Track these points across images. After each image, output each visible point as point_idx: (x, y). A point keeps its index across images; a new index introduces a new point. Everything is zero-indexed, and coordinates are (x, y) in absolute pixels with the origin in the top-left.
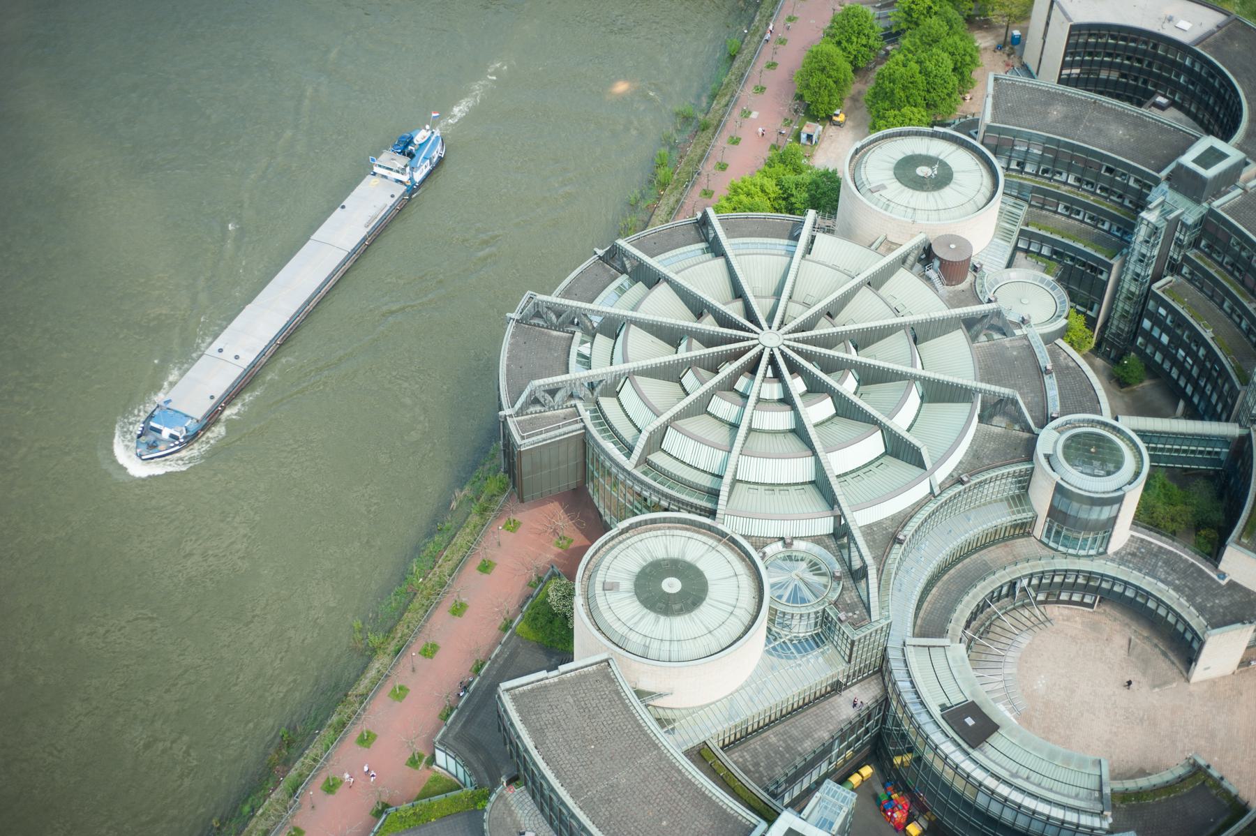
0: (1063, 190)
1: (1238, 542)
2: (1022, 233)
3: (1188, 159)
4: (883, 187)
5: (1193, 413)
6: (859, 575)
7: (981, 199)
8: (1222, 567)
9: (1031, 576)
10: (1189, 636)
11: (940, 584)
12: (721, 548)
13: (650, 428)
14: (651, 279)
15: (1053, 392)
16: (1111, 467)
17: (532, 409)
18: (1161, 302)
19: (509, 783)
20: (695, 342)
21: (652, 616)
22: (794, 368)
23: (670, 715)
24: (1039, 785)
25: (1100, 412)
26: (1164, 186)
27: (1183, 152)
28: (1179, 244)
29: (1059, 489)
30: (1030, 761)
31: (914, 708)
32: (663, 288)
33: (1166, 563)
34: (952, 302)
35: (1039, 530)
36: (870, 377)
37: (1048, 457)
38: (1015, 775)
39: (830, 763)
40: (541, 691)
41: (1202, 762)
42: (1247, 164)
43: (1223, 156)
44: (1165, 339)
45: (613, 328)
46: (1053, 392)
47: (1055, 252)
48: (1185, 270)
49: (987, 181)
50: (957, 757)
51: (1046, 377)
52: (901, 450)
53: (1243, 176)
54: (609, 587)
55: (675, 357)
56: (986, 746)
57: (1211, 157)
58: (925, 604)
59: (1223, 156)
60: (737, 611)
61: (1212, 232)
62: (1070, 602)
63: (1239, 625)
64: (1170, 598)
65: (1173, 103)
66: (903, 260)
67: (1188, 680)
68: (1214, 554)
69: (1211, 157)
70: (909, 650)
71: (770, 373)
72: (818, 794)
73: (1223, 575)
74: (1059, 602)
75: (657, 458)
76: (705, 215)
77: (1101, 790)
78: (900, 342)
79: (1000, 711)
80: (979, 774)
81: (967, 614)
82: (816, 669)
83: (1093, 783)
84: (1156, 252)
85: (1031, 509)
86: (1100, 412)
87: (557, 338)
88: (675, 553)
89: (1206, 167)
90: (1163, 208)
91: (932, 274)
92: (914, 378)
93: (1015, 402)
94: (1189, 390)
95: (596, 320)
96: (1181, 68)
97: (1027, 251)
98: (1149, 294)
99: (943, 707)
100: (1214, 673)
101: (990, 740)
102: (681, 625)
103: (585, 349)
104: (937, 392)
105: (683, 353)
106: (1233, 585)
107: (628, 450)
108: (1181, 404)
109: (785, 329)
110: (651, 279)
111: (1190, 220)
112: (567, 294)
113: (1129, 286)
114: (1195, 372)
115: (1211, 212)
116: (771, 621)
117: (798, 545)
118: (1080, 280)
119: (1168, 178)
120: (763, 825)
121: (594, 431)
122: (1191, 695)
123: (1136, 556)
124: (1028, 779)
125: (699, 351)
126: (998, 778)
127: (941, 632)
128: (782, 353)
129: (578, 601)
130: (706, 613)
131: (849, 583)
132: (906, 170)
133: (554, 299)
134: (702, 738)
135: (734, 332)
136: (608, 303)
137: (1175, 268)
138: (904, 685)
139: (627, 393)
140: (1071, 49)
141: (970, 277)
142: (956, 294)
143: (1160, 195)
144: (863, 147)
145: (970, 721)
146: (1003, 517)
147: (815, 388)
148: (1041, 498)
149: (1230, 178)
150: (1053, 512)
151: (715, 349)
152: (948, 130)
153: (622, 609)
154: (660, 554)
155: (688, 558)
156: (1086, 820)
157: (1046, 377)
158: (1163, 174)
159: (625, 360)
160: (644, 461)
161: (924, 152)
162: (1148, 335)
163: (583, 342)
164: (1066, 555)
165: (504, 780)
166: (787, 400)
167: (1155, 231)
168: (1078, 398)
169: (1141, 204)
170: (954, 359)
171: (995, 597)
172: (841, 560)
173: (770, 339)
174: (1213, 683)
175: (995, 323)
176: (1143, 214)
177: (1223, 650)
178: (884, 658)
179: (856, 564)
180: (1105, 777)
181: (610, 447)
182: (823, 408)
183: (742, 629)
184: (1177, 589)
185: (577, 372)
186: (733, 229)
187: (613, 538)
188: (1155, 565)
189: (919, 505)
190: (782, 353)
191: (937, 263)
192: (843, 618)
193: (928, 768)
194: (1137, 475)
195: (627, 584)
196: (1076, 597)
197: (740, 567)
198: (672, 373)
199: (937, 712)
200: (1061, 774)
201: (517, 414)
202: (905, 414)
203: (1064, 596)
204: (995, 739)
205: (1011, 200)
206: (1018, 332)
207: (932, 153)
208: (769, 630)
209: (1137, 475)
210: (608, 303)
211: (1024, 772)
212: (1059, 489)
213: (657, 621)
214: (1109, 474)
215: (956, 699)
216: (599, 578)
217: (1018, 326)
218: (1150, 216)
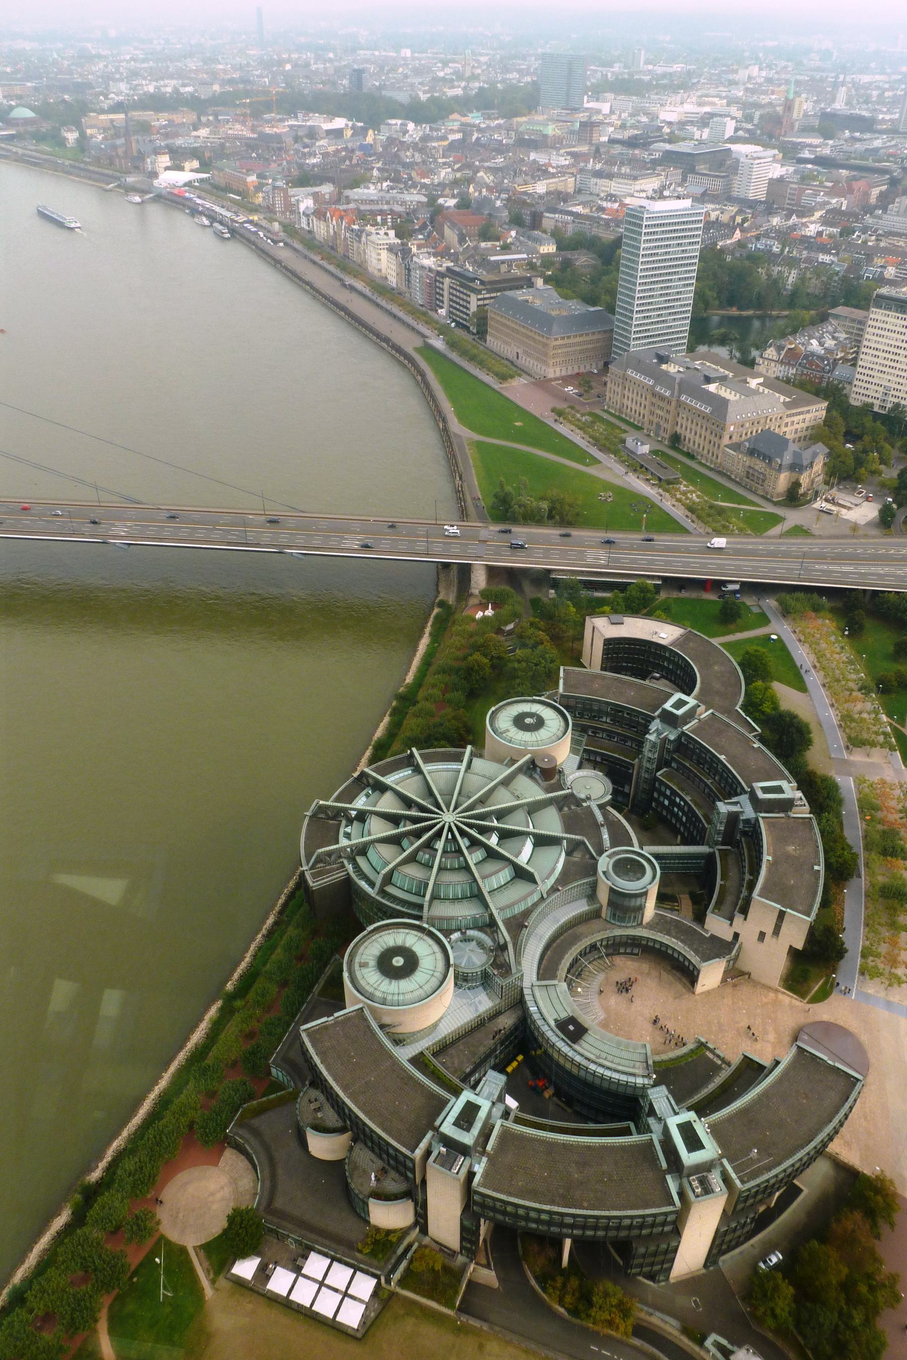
0: (605, 726)
1: (713, 912)
2: (585, 750)
3: (668, 706)
4: (508, 731)
5: (685, 842)
6: (503, 948)
7: (560, 733)
8: (706, 926)
9: (602, 940)
10: (691, 968)
11: (551, 949)
12: (426, 938)
13: (383, 872)
14: (382, 788)
15: (606, 836)
16: (639, 875)
17: (319, 865)
18: (662, 783)
19: (310, 1085)
20: (408, 822)
21: (387, 981)
22: (463, 833)
23: (401, 1037)
24: (612, 1062)
25: (632, 846)
26: (657, 721)
27: (666, 701)
28: (668, 751)
29: (611, 890)
30: (606, 1048)
31: (540, 1023)
32: (388, 795)
33: (676, 926)
34: (548, 790)
35: (605, 912)
36: (505, 835)
37: (604, 873)
38: (598, 1057)
39: (496, 1058)
40: (324, 1028)
41: (703, 1040)
43: (686, 703)
44: (666, 802)
45: (362, 817)
46: (606, 836)
47: (602, 759)
48: (674, 765)
49: (562, 723)
50: (565, 1049)
51: (602, 828)
52: (521, 874)
53: (698, 713)
54: (364, 965)
55: (397, 831)
56: (582, 1042)
58: (544, 962)
59: (686, 703)
60: (436, 974)
61: (684, 746)
62: (625, 953)
63: (717, 960)
64: (679, 947)
65: (662, 677)
66: (520, 770)
67: (694, 993)
68: (700, 918)
69: (680, 704)
70: (536, 990)
71: (450, 836)
72: (484, 1078)
73: (707, 931)
74: (619, 954)
75: (390, 889)
76: (412, 753)
77: (647, 1062)
78: (520, 815)
79: (585, 1020)
80: (578, 1058)
81: (568, 965)
82: (483, 1003)
83: (643, 1059)
84: (656, 756)
85: (599, 902)
86: (632, 846)
87: (333, 824)
88: (399, 942)
89: (678, 709)
90: (656, 732)
91: (537, 777)
92: (527, 834)
93: (584, 843)
94: (682, 829)
95: (354, 813)
96: (665, 658)
97: (588, 760)
98: (656, 779)
99: (556, 1021)
100: (705, 988)
101: (585, 1037)
102: (406, 985)
103: (348, 830)
104: (542, 841)
105: (402, 829)
106: (713, 937)
107: (372, 884)
108: (679, 837)
109: (459, 809)
110: (382, 788)
111: (672, 737)
112: (336, 800)
113: (644, 775)
114: (684, 819)
115: (683, 733)
116: (456, 977)
117: (470, 933)
118: (617, 773)
119: (659, 716)
120: (453, 1099)
121: (353, 876)
122: (696, 1001)
123: (659, 924)
124: (606, 1059)
125: (410, 827)
126: (589, 1060)
127: (554, 977)
128: (455, 825)
129: (346, 975)
130: (419, 976)
131: (499, 953)
132: (519, 722)
133: (329, 803)
134: (420, 1050)
135: (429, 815)
136: (361, 802)
137: (667, 764)
138: (533, 1009)
139: (371, 853)
140: (606, 652)
141: (557, 777)
142: (551, 785)
143: (655, 725)
144: (496, 710)
145: (571, 1028)
146: (581, 907)
147: (475, 843)
148: (603, 896)
149: (691, 714)
150: (610, 903)
151: (418, 825)
152: (542, 698)
153: (371, 978)
154: (391, 943)
155: (407, 945)
156: (640, 1081)
157: (602, 828)
158: (657, 713)
159: (370, 835)
160: (382, 892)
161: (528, 711)
162: (657, 800)
163: (347, 826)
164: (620, 927)
165: (307, 1083)
166: (459, 851)
167: (654, 745)
168: (620, 838)
169: (647, 731)
170: (551, 823)
171: (583, 954)
172: (494, 940)
173: (449, 818)
174: (708, 993)
175: (571, 799)
176: (647, 736)
177: (711, 975)
178: (522, 995)
179: (502, 942)
180: (649, 1053)
181: (363, 884)
182: (479, 855)
183: (438, 983)
184: (682, 941)
185: (344, 842)
186: (427, 759)
187: (364, 937)
188: (670, 930)
189: (535, 905)
190: (455, 825)
191: (538, 770)
192: (496, 973)
193: (550, 1057)
194: (654, 877)
195: (373, 963)
196: (628, 950)
197: (436, 948)
198: (395, 841)
199: (552, 1023)
200: (624, 1054)
201: (311, 869)
202: (525, 853)
203: (622, 951)
204: (586, 1037)
205: (577, 733)
206: (585, 804)
207: (533, 710)
208: (456, 984)
209: (654, 877)
210: (361, 802)
211: (604, 1055)
212: (611, 890)
213: (390, 983)
214: (638, 879)
215: (563, 1015)
216: (357, 960)
217: (584, 801)
218: (652, 737)
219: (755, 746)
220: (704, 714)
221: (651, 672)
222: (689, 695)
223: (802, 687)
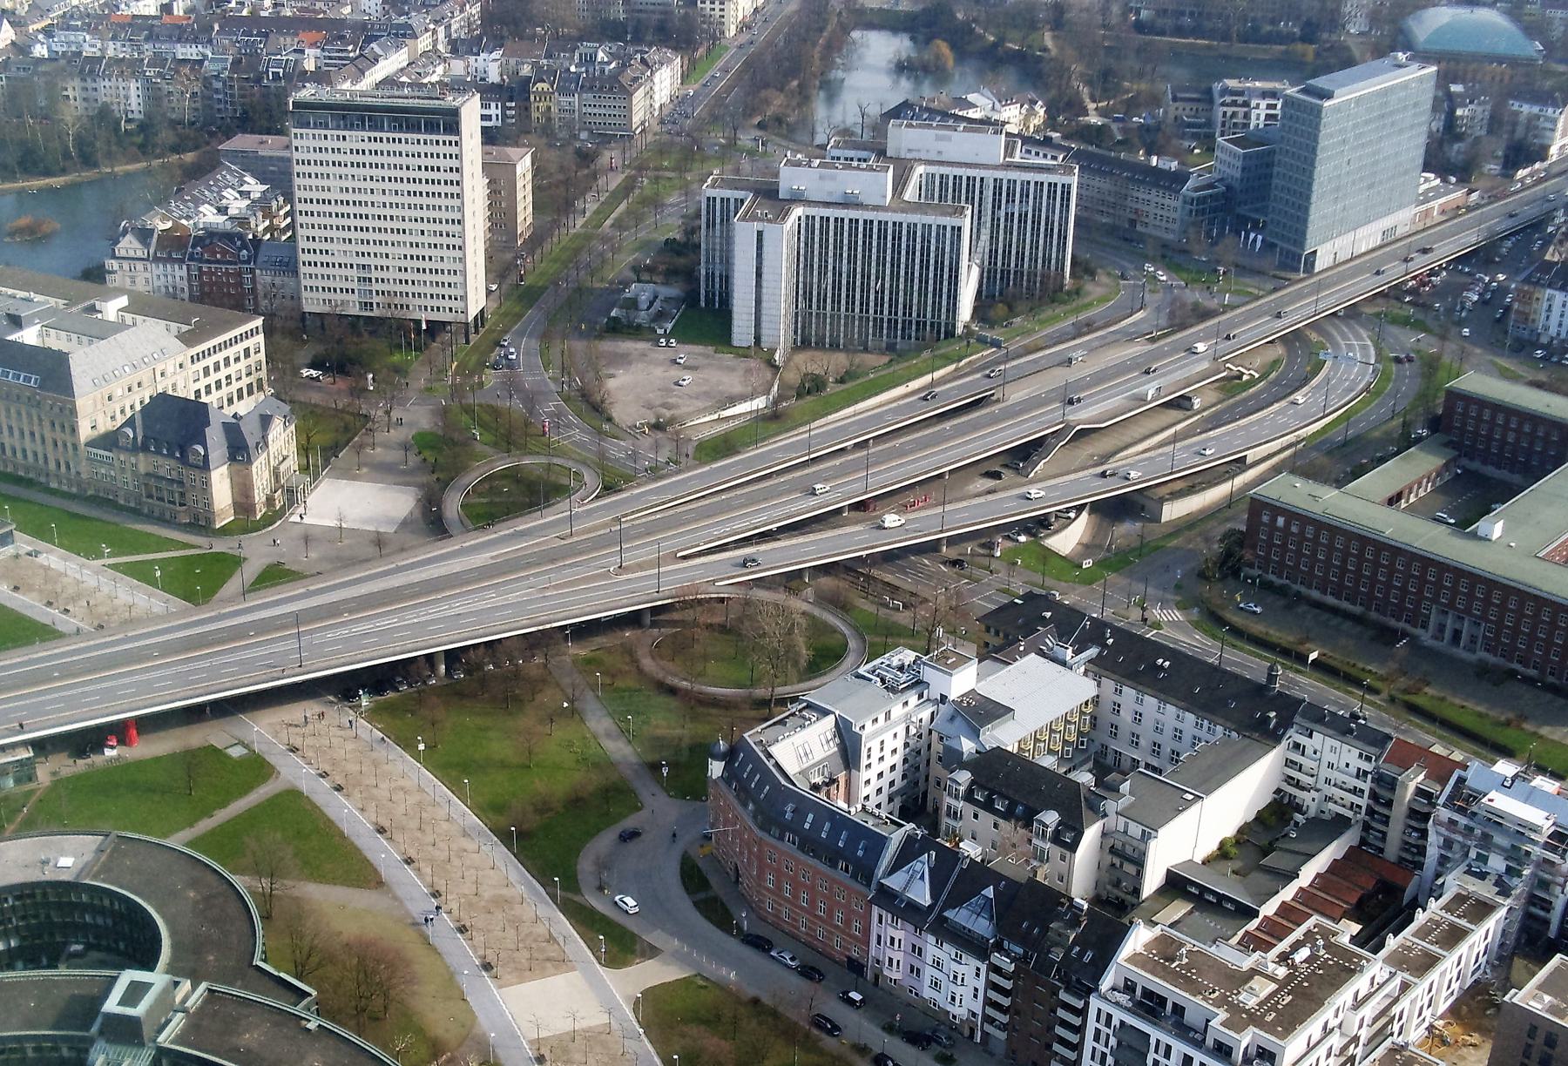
3: (111, 1005)
42: (176, 984)
43: (146, 987)
57: (135, 992)
59: (146, 987)
69: (135, 992)
89: (134, 1005)
119: (101, 1033)
149: (165, 1004)
219: (312, 1026)
220: (192, 994)
221: (66, 944)
222: (151, 968)
223: (364, 875)
